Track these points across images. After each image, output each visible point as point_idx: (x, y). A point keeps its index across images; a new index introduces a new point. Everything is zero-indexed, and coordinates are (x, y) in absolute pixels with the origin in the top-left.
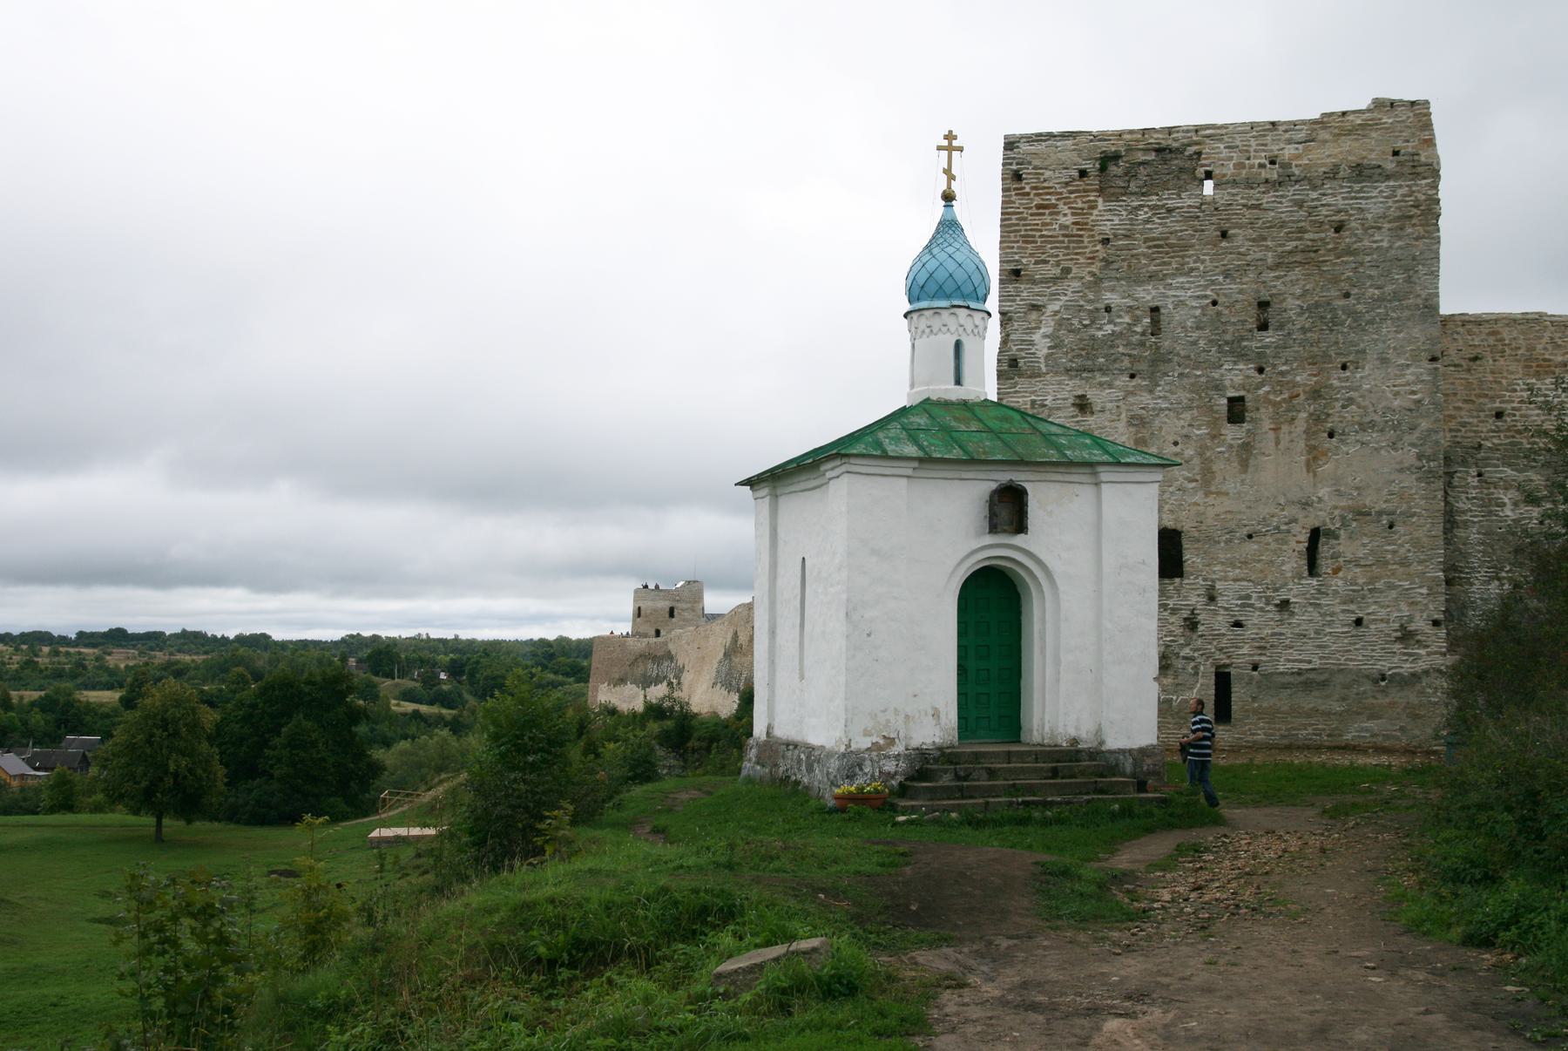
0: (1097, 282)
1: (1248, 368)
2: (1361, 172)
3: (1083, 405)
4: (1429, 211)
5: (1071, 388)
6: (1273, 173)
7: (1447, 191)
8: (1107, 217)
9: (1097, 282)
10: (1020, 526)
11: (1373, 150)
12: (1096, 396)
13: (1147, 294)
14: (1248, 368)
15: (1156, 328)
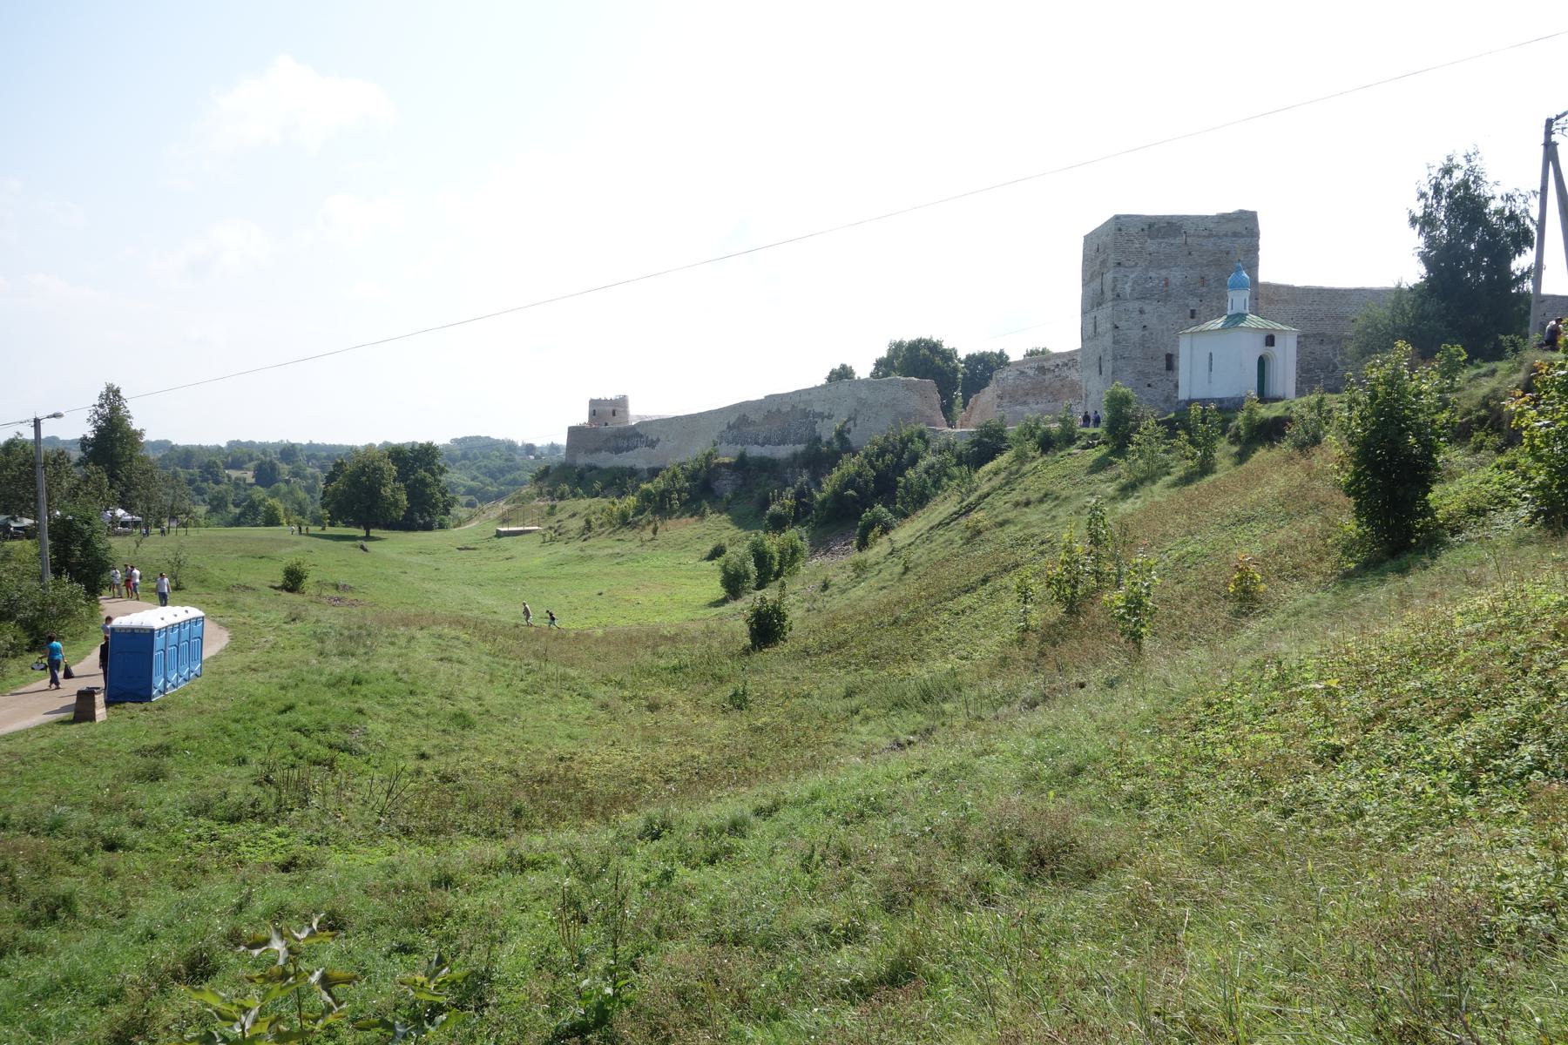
0: (1146, 269)
1: (1197, 300)
2: (1235, 234)
3: (1142, 312)
4: (1256, 248)
5: (1137, 304)
6: (1206, 233)
7: (1262, 243)
8: (1151, 245)
9: (1146, 269)
10: (1273, 345)
11: (1239, 227)
12: (1147, 308)
13: (1164, 273)
14: (1197, 300)
15: (1167, 284)
